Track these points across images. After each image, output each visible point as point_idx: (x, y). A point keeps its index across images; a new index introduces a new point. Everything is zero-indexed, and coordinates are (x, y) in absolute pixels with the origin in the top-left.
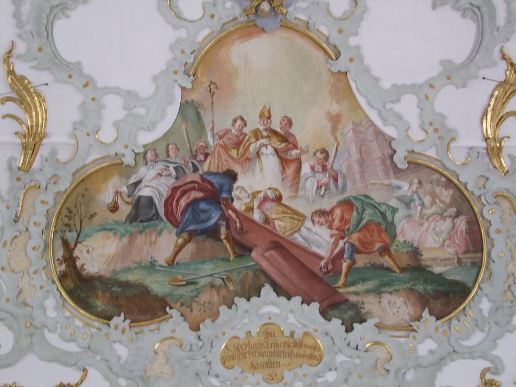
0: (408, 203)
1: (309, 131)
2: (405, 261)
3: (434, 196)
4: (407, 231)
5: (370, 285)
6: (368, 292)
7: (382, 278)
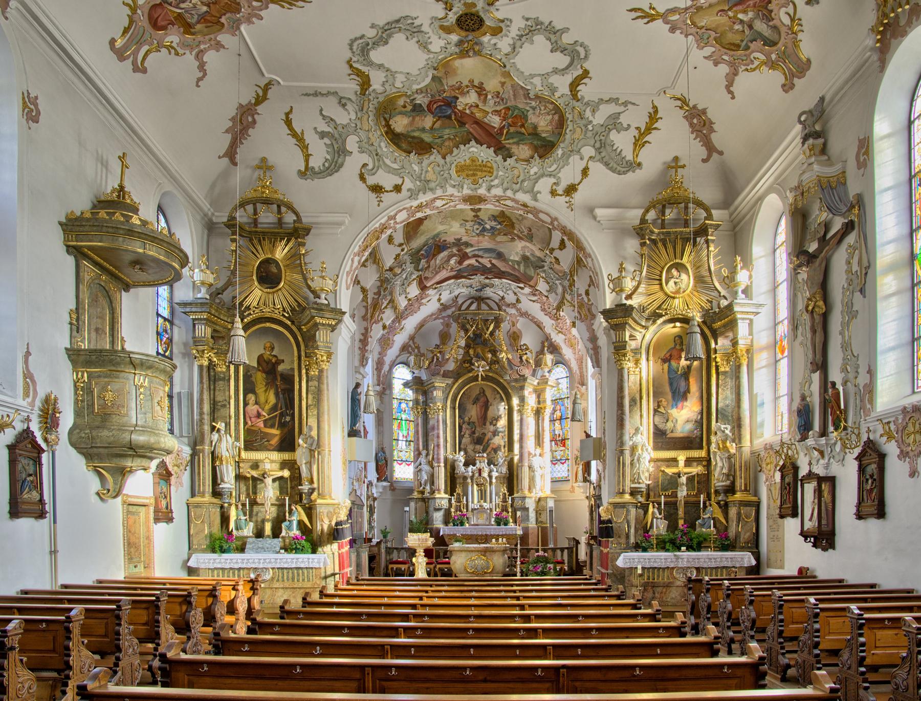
0: (534, 109)
1: (492, 85)
2: (530, 131)
3: (546, 107)
4: (532, 118)
5: (515, 140)
6: (514, 143)
7: (520, 138)
